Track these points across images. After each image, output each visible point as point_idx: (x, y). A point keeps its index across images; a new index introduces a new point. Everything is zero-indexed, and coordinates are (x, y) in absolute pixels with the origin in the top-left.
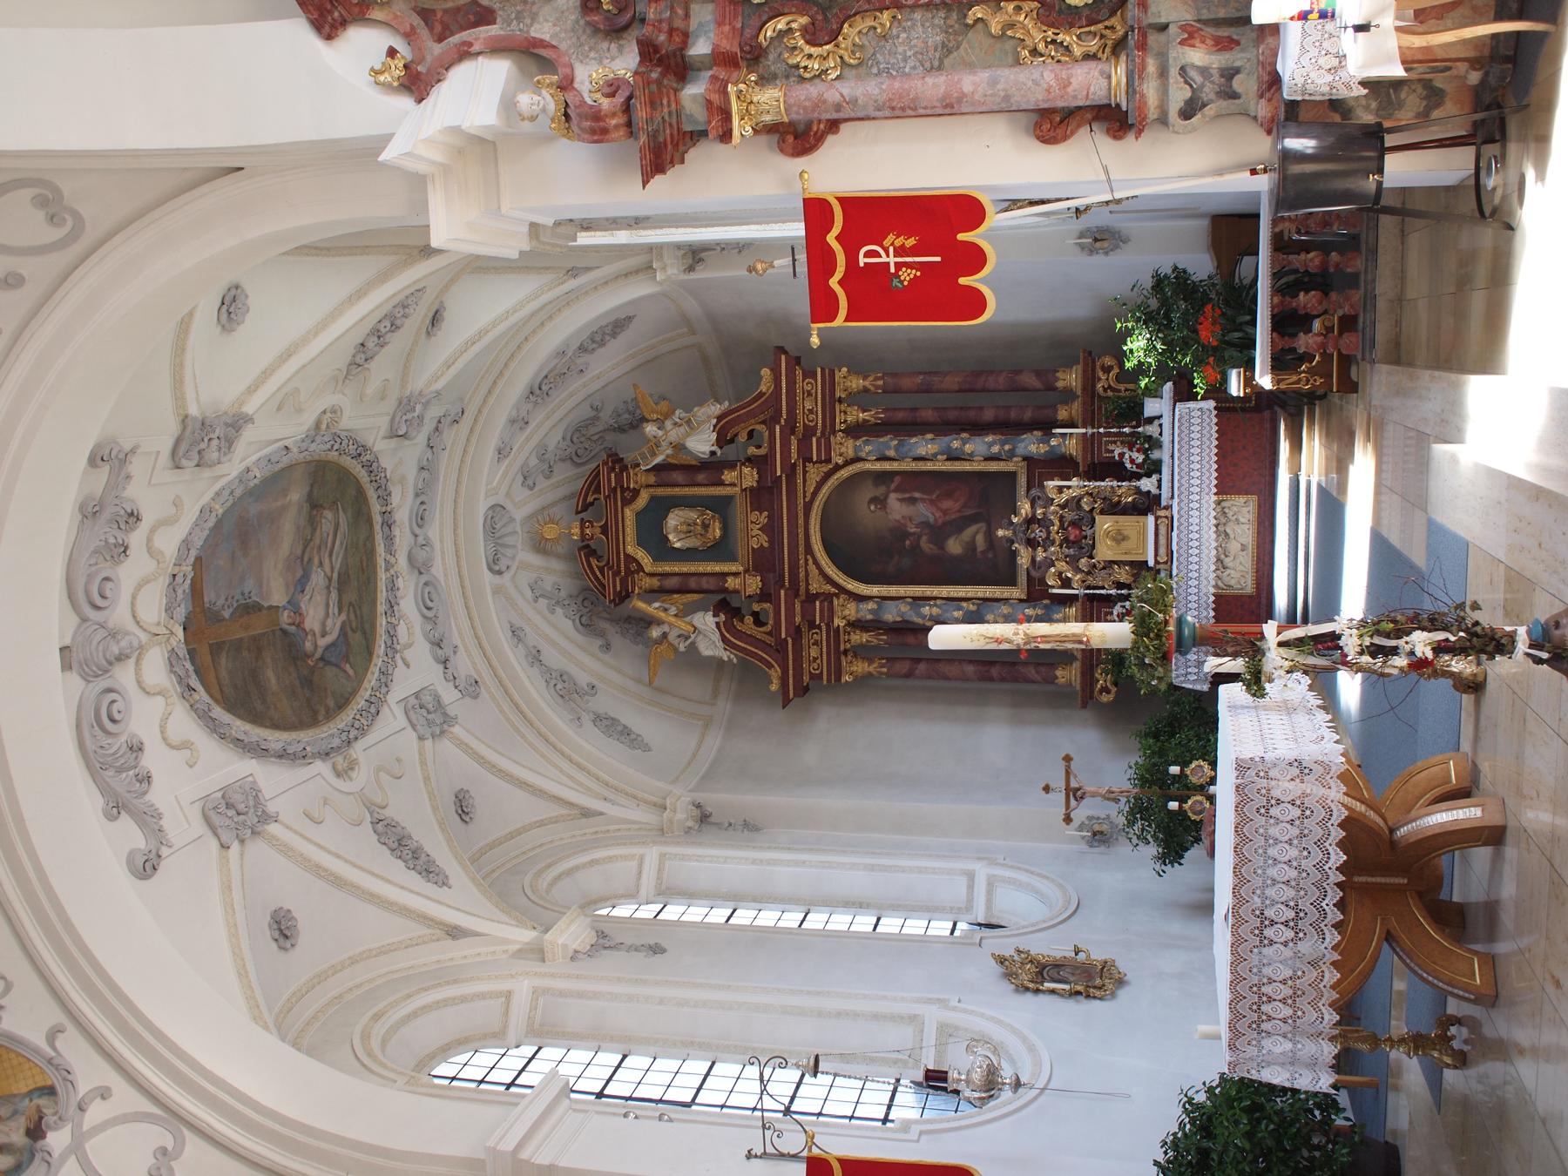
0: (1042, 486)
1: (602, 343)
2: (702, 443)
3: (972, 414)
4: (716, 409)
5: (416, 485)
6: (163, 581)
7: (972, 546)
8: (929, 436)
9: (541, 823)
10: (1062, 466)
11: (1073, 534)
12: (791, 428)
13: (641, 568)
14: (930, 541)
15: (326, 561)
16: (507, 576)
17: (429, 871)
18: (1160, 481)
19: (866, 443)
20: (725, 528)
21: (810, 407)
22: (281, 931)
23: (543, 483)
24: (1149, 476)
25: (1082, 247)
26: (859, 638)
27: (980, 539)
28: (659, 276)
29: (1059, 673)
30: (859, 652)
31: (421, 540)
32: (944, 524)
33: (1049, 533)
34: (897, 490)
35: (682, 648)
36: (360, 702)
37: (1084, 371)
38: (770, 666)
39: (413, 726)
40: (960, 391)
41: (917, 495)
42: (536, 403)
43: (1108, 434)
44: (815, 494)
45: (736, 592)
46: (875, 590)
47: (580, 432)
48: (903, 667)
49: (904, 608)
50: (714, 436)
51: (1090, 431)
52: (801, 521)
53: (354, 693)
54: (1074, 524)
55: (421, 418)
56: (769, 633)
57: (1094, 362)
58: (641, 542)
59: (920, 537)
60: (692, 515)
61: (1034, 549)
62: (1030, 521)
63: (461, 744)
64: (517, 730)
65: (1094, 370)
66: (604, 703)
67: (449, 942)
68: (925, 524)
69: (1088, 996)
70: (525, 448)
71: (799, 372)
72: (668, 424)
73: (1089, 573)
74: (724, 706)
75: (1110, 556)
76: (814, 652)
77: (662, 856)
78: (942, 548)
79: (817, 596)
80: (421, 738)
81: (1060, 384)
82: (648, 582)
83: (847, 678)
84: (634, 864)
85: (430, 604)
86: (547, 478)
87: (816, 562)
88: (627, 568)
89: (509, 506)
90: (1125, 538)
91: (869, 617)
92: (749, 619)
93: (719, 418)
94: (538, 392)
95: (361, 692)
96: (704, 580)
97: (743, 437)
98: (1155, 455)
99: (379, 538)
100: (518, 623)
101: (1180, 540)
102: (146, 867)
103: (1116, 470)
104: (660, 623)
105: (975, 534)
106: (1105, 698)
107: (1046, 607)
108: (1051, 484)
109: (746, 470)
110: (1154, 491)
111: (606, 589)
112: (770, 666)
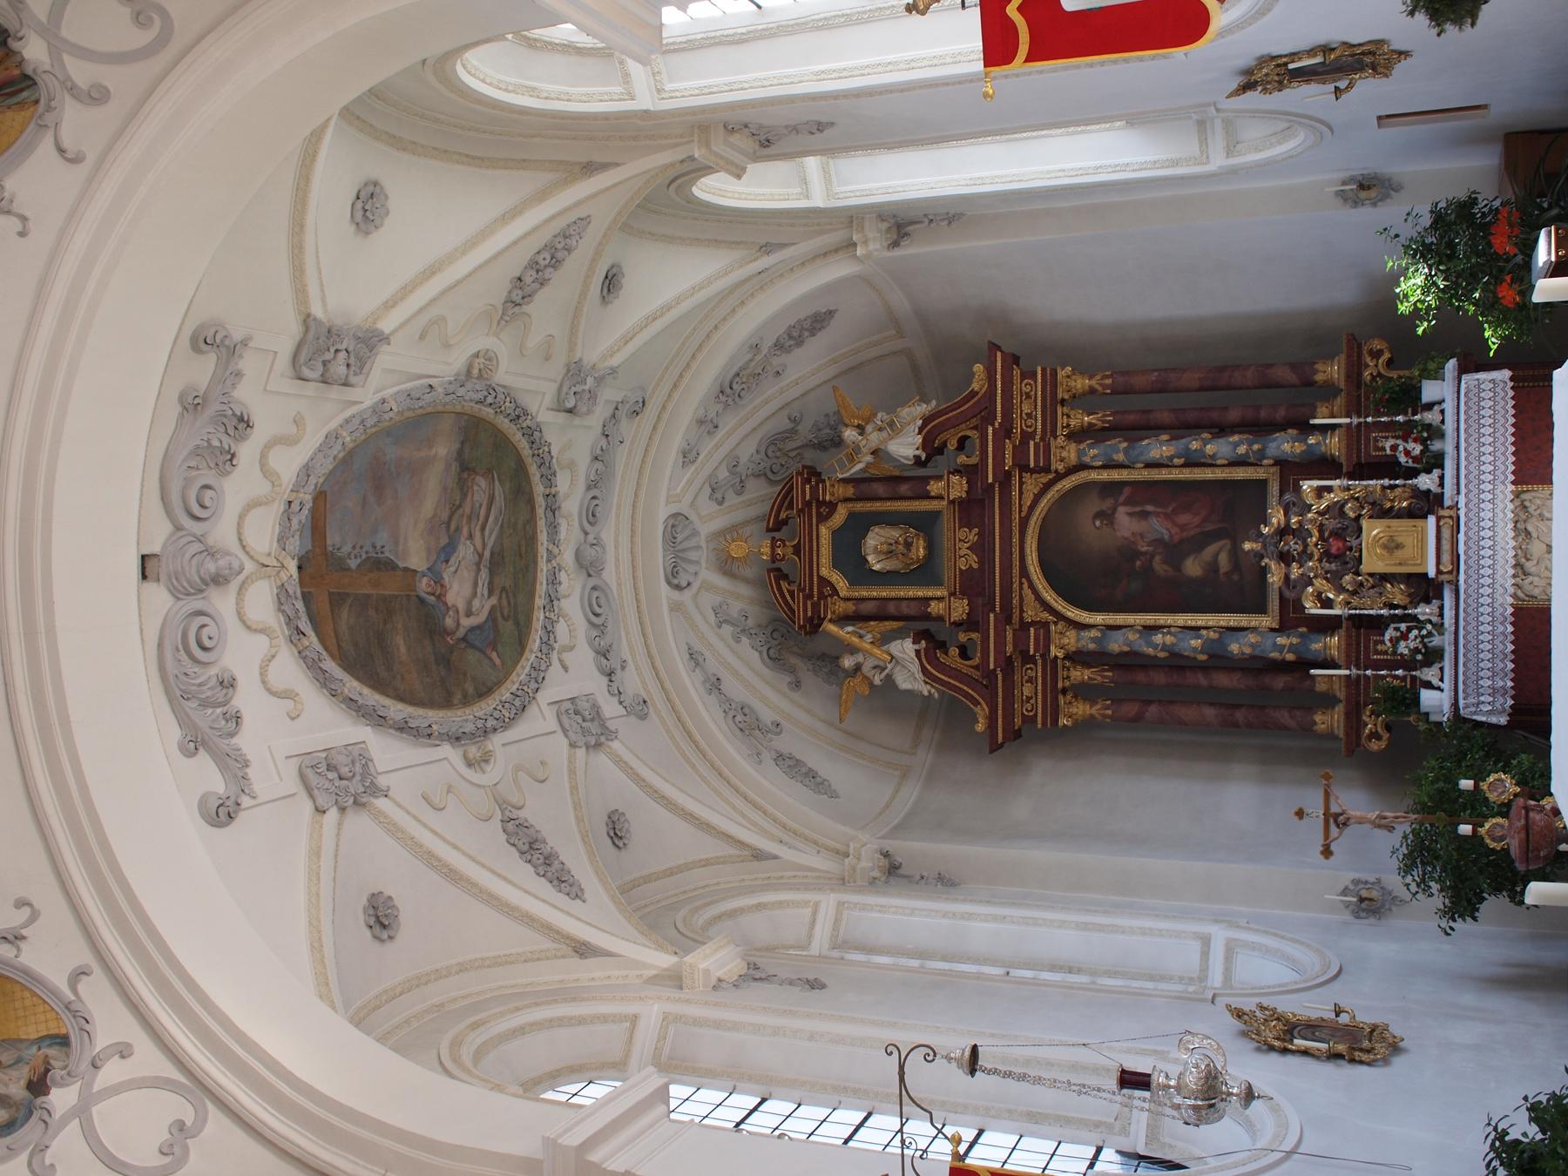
0: (1298, 489)
1: (799, 342)
2: (906, 447)
3: (1215, 415)
4: (924, 409)
5: (588, 476)
6: (278, 508)
7: (1213, 567)
8: (1165, 437)
9: (707, 863)
10: (1324, 466)
11: (1335, 546)
12: (1006, 431)
13: (835, 592)
14: (1164, 562)
15: (478, 534)
16: (687, 596)
17: (561, 880)
18: (1442, 478)
19: (1090, 446)
20: (931, 547)
21: (1028, 411)
23: (732, 499)
24: (1429, 472)
25: (1341, 194)
26: (1079, 674)
27: (1223, 559)
28: (860, 251)
29: (1318, 718)
30: (1083, 692)
31: (591, 538)
32: (1181, 541)
33: (1306, 546)
34: (1124, 504)
35: (877, 681)
36: (504, 693)
37: (1349, 356)
38: (977, 703)
39: (565, 731)
40: (1201, 389)
41: (1149, 508)
42: (727, 405)
43: (1377, 426)
44: (1032, 508)
45: (940, 618)
46: (1099, 618)
47: (775, 444)
48: (1130, 709)
49: (1132, 636)
50: (919, 439)
51: (1355, 421)
52: (1016, 540)
53: (499, 683)
54: (1338, 534)
55: (592, 396)
56: (976, 668)
57: (1360, 347)
58: (837, 564)
59: (1152, 556)
60: (894, 533)
61: (1288, 565)
62: (1283, 532)
63: (619, 761)
64: (687, 760)
65: (1360, 356)
66: (788, 743)
67: (576, 960)
68: (1158, 542)
69: (1352, 1061)
70: (714, 453)
71: (1016, 372)
72: (869, 428)
73: (1354, 593)
74: (924, 757)
75: (1380, 567)
76: (1027, 690)
77: (841, 904)
78: (1178, 568)
79: (1033, 623)
80: (573, 745)
81: (1319, 377)
82: (842, 607)
83: (1063, 721)
84: (808, 912)
85: (598, 610)
86: (739, 494)
87: (1032, 586)
88: (820, 592)
89: (693, 517)
90: (1399, 546)
91: (1092, 646)
92: (954, 651)
93: (927, 420)
94: (732, 390)
95: (508, 684)
96: (904, 604)
97: (952, 445)
98: (1436, 446)
99: (541, 523)
100: (697, 646)
101: (1468, 539)
102: (221, 814)
103: (1388, 468)
104: (853, 650)
105: (1219, 553)
106: (1375, 746)
107: (1302, 635)
108: (1307, 485)
109: (955, 479)
110: (1434, 488)
111: (797, 623)
112: (977, 703)
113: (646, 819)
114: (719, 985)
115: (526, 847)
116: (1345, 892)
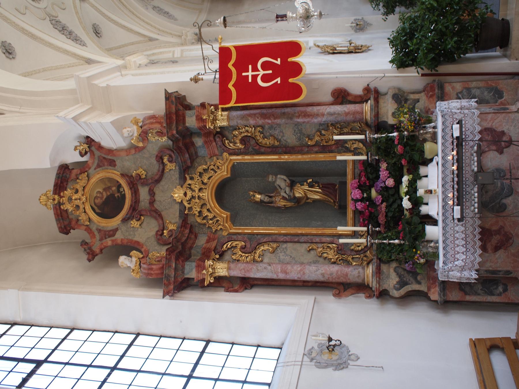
9: (132, 44)
17: (76, 40)
22: (6, 50)
67: (87, 66)
69: (356, 52)
77: (182, 51)
113: (106, 27)
114: (140, 66)
115: (61, 29)
116: (352, 23)
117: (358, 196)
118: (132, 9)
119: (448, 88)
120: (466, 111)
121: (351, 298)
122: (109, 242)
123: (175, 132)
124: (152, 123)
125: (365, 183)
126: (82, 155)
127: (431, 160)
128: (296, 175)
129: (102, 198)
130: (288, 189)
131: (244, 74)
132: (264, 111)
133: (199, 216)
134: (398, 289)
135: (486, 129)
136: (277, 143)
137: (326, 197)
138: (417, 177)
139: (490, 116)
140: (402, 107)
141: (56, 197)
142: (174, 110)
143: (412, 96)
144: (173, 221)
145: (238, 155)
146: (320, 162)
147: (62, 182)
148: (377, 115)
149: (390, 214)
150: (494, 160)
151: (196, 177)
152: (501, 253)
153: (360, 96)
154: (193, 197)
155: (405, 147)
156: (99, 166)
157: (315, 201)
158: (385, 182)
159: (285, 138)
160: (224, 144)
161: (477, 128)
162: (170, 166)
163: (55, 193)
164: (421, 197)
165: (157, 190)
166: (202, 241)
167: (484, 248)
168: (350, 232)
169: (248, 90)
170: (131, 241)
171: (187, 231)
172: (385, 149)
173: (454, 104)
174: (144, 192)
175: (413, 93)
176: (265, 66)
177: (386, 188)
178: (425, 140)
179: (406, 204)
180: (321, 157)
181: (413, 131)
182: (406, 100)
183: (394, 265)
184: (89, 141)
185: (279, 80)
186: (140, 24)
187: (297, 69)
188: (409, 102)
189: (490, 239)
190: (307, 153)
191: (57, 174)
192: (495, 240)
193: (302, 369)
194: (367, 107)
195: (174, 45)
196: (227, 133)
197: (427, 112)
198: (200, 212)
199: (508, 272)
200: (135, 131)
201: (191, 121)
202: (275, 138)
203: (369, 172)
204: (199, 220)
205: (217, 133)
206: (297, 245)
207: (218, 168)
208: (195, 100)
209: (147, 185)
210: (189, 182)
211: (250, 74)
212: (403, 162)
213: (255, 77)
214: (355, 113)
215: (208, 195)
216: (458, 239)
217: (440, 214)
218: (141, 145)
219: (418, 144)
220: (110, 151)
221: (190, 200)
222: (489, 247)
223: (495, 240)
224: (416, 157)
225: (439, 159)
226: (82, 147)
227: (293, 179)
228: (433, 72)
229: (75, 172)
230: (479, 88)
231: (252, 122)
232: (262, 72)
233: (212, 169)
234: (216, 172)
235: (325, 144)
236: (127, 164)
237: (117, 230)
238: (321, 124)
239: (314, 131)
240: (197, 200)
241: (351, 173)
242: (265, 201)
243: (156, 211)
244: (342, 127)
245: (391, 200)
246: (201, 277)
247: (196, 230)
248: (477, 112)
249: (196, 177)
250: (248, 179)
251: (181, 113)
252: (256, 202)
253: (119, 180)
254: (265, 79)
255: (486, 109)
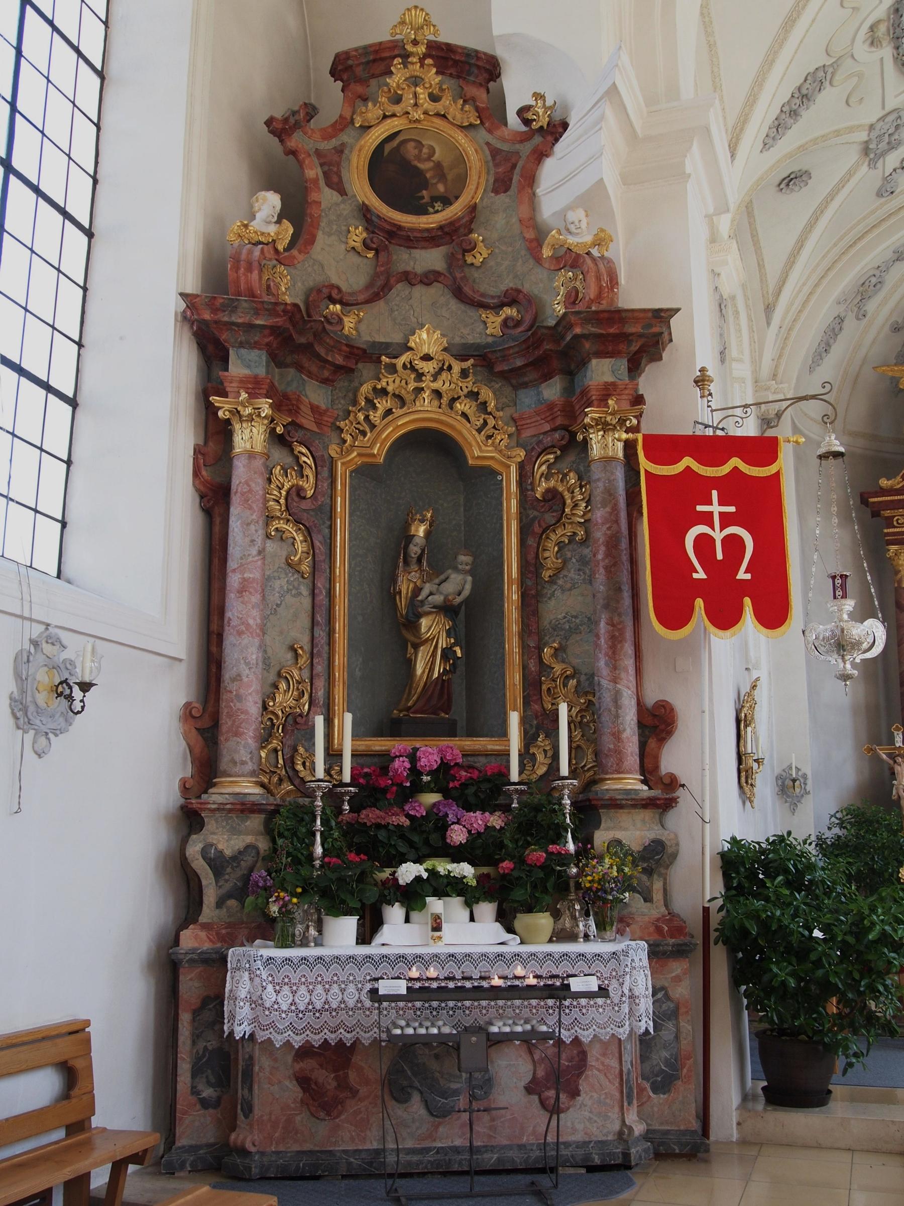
17: (779, 127)
39: (882, 119)
63: (850, 174)
64: (841, 239)
77: (743, 380)
80: (872, 127)
113: (802, 202)
114: (715, 274)
115: (804, 91)
117: (423, 762)
118: (839, 265)
119: (677, 967)
120: (625, 1008)
121: (181, 745)
122: (313, 171)
123: (578, 330)
124: (598, 278)
125: (454, 778)
126: (521, 112)
127: (510, 930)
128: (472, 619)
129: (418, 157)
130: (438, 599)
131: (715, 494)
132: (624, 544)
133: (374, 389)
134: (204, 853)
135: (583, 1055)
136: (546, 574)
137: (419, 690)
138: (470, 896)
139: (614, 1063)
140: (634, 864)
141: (422, 49)
142: (631, 329)
143: (658, 885)
144: (363, 327)
145: (521, 483)
146: (503, 675)
147: (456, 63)
148: (615, 804)
149: (382, 835)
150: (512, 1071)
151: (468, 385)
152: (292, 1091)
153: (657, 767)
154: (420, 376)
155: (542, 867)
156: (495, 152)
157: (410, 665)
158: (458, 823)
159: (558, 593)
160: (545, 450)
161: (586, 1033)
162: (494, 323)
163: (431, 45)
164: (424, 905)
165: (436, 292)
166: (315, 394)
167: (305, 1051)
168: (338, 742)
169: (677, 503)
170: (315, 225)
171: (339, 360)
172: (537, 822)
173: (640, 979)
174: (431, 259)
175: (665, 890)
176: (733, 543)
177: (443, 827)
178: (556, 915)
179: (408, 872)
180: (514, 678)
181: (578, 886)
182: (649, 872)
183: (263, 845)
184: (556, 129)
185: (700, 575)
186: (804, 284)
187: (725, 618)
188: (644, 878)
189: (327, 1067)
190: (524, 646)
191: (477, 51)
192: (325, 1078)
193: (13, 618)
194: (632, 782)
195: (756, 362)
196: (571, 458)
197: (621, 920)
198: (384, 392)
199: (248, 1110)
200: (581, 238)
201: (602, 371)
202: (559, 570)
203: (482, 787)
204: (366, 389)
205: (573, 435)
206: (305, 621)
207: (489, 437)
208: (649, 382)
209: (450, 266)
210: (457, 367)
211: (716, 508)
212: (506, 865)
213: (707, 519)
214: (619, 753)
215: (425, 411)
216: (327, 991)
217: (385, 951)
218: (546, 252)
219: (547, 899)
220: (531, 180)
221: (413, 369)
222: (309, 1064)
223: (325, 1078)
224: (519, 894)
225: (513, 946)
226: (541, 111)
227: (462, 615)
228: (713, 935)
229: (481, 94)
230: (677, 1037)
231: (599, 515)
232: (718, 536)
233: (485, 423)
234: (479, 431)
235: (544, 687)
236: (500, 220)
237: (342, 192)
238: (591, 676)
239: (576, 661)
240: (412, 385)
241: (477, 747)
242: (411, 545)
243: (386, 288)
244: (587, 723)
245: (416, 838)
246: (230, 387)
247: (342, 383)
248: (623, 1033)
249: (468, 385)
250: (462, 509)
251: (622, 347)
252: (407, 526)
253: (460, 200)
254: (704, 542)
255: (631, 1053)
